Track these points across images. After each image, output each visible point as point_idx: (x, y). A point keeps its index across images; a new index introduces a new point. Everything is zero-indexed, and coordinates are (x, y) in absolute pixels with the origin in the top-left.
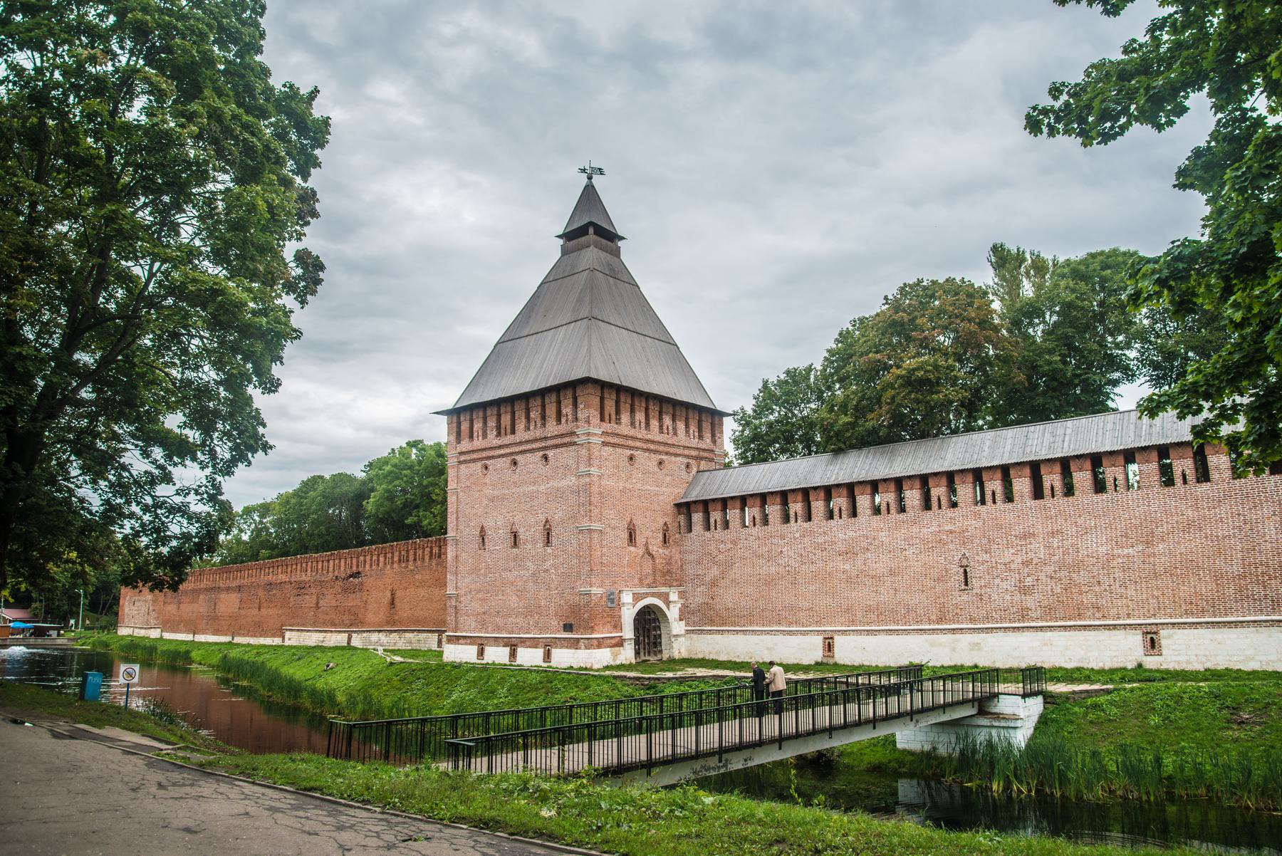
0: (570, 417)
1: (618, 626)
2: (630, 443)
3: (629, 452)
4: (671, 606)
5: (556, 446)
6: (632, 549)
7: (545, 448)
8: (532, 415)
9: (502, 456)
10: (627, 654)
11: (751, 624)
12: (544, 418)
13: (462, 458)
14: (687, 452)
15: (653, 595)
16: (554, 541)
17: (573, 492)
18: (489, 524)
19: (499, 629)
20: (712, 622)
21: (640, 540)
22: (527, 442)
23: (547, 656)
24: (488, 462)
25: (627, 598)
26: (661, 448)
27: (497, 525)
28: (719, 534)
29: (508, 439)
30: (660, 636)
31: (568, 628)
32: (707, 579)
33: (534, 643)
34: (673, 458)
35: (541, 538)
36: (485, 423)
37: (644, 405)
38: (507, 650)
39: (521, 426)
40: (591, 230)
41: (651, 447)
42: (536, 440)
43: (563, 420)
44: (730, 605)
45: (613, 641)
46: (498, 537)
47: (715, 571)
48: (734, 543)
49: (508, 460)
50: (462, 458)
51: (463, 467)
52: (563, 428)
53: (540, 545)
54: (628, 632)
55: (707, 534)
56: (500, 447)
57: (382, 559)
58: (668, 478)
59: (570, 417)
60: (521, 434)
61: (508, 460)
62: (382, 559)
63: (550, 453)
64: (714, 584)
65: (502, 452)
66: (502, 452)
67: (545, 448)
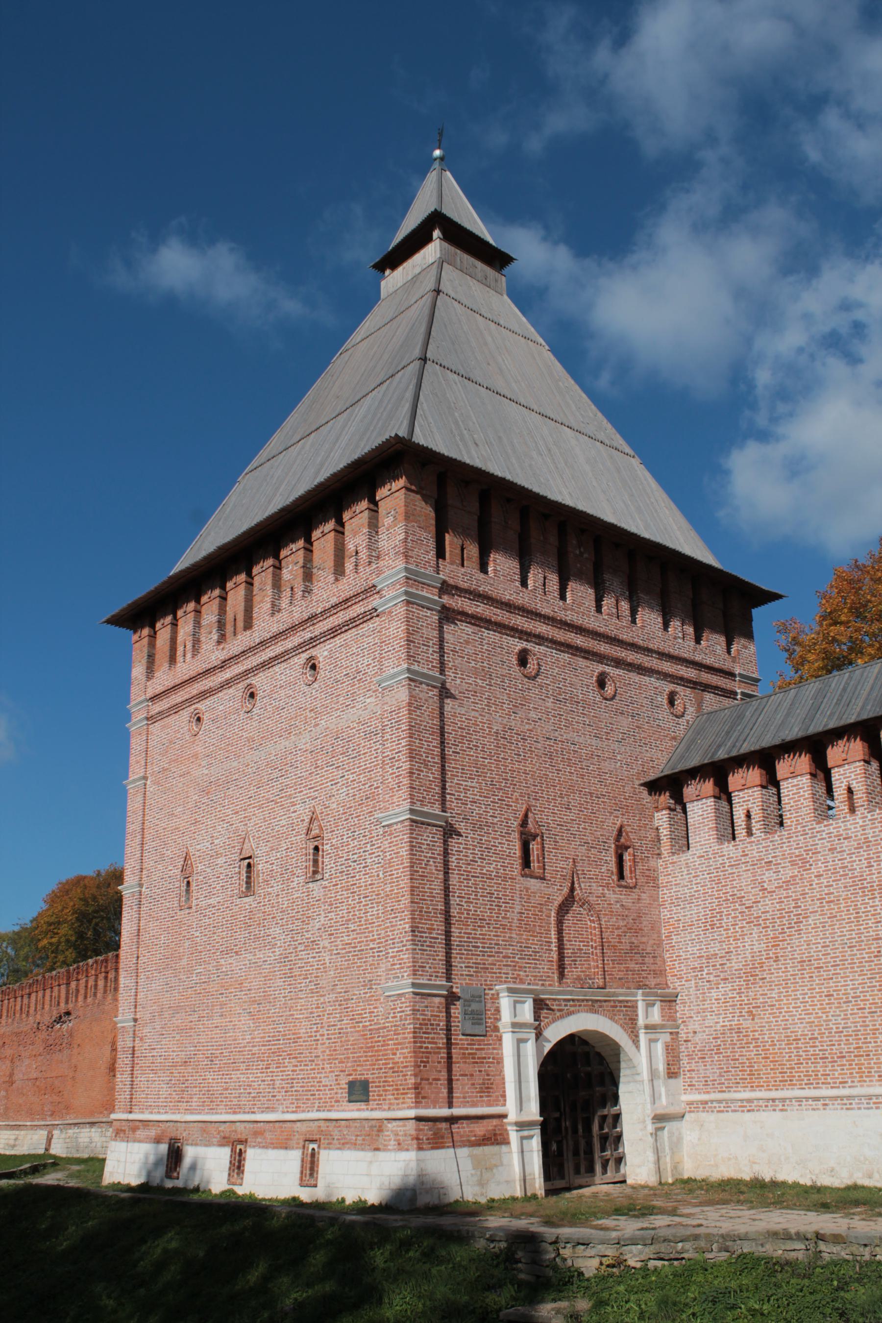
0: (363, 555)
1: (491, 1088)
2: (519, 621)
3: (518, 645)
4: (643, 1038)
5: (334, 632)
6: (533, 884)
7: (313, 642)
8: (286, 574)
9: (227, 684)
10: (518, 1166)
11: (863, 1076)
12: (308, 576)
13: (157, 708)
14: (667, 667)
15: (594, 1006)
16: (328, 863)
17: (369, 735)
18: (199, 847)
19: (211, 1102)
20: (752, 1079)
21: (557, 864)
22: (276, 637)
23: (310, 1169)
24: (201, 706)
25: (511, 1010)
26: (603, 648)
27: (214, 849)
28: (756, 845)
29: (244, 640)
30: (617, 1117)
31: (359, 1091)
32: (735, 964)
33: (279, 1137)
34: (635, 677)
35: (301, 863)
36: (197, 623)
37: (553, 539)
38: (225, 1153)
39: (262, 607)
40: (436, 233)
41: (579, 643)
42: (293, 628)
43: (349, 566)
44: (800, 1029)
45: (480, 1129)
46: (218, 876)
47: (754, 943)
48: (802, 863)
49: (236, 692)
50: (157, 708)
51: (155, 728)
52: (349, 584)
53: (298, 881)
54: (519, 1097)
55: (728, 848)
56: (224, 665)
57: (101, 983)
58: (625, 722)
59: (363, 555)
60: (265, 624)
61: (236, 692)
62: (101, 983)
63: (321, 653)
64: (752, 974)
65: (227, 674)
66: (227, 674)
67: (313, 642)
